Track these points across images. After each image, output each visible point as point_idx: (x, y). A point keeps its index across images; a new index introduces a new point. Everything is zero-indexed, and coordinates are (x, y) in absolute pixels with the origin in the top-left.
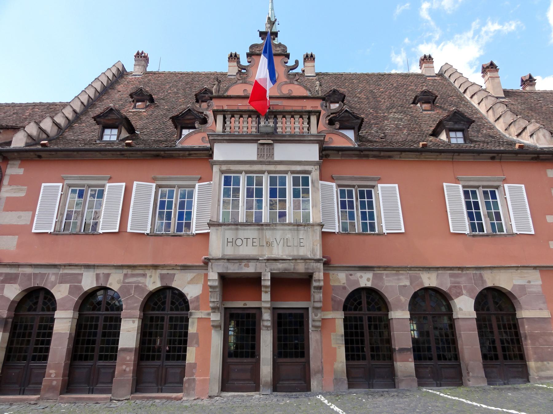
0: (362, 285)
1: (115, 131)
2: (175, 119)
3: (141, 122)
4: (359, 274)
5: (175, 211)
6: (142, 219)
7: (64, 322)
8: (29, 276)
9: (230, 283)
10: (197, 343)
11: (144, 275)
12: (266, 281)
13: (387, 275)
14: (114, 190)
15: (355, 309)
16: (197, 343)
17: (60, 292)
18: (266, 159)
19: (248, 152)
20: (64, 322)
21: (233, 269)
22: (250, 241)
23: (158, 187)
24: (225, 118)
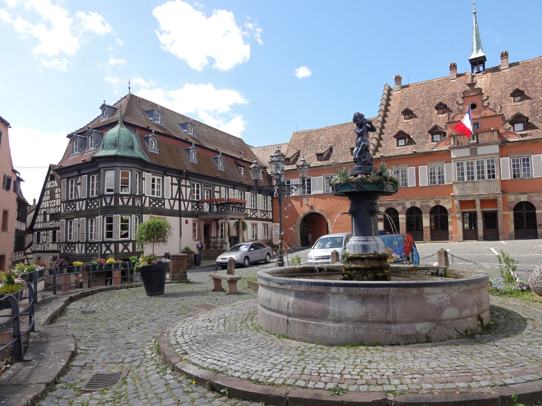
0: (522, 200)
1: (403, 140)
2: (430, 132)
3: (411, 129)
4: (521, 196)
5: (437, 176)
6: (424, 181)
7: (402, 218)
8: (386, 204)
9: (463, 203)
10: (452, 224)
11: (428, 201)
12: (478, 202)
13: (534, 196)
14: (411, 171)
15: (520, 210)
16: (452, 224)
17: (399, 209)
18: (474, 152)
19: (466, 152)
20: (402, 218)
21: (464, 199)
22: (470, 188)
23: (428, 166)
24: (454, 138)
